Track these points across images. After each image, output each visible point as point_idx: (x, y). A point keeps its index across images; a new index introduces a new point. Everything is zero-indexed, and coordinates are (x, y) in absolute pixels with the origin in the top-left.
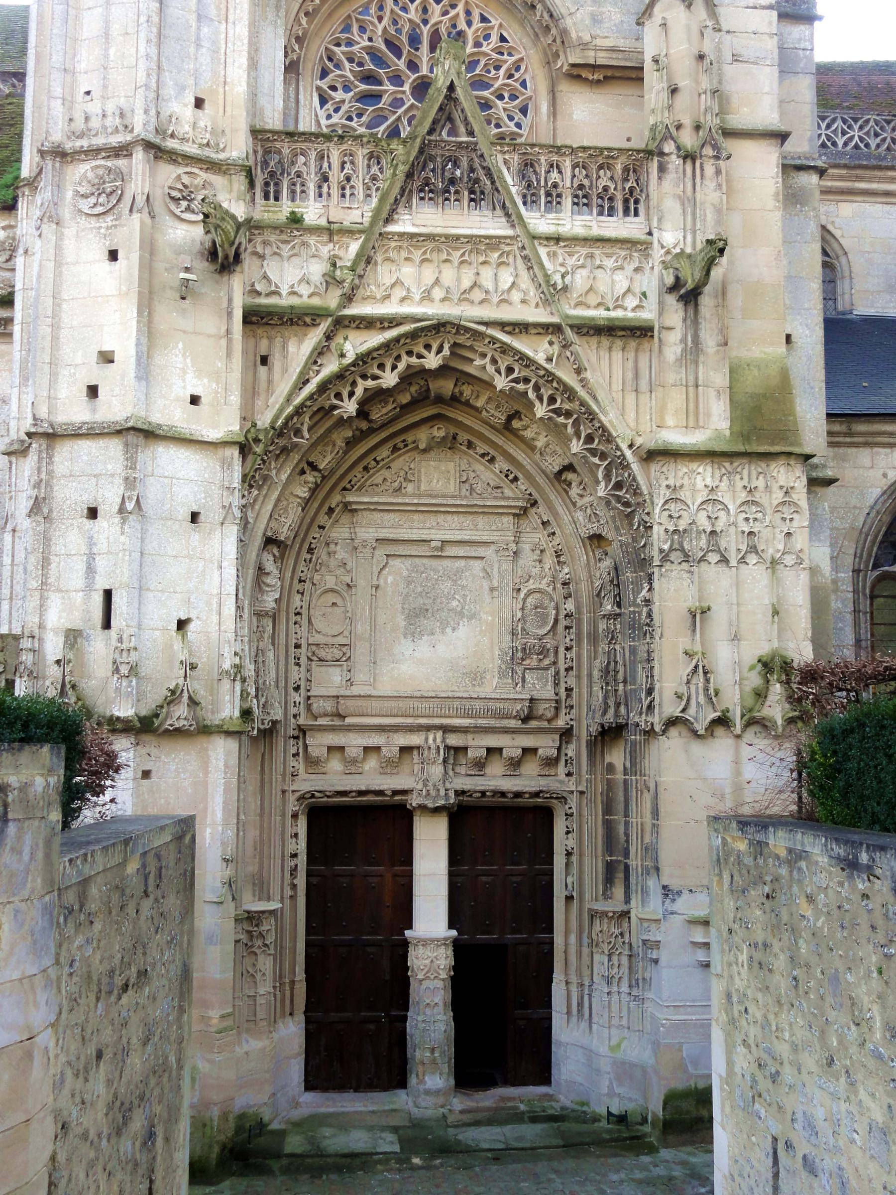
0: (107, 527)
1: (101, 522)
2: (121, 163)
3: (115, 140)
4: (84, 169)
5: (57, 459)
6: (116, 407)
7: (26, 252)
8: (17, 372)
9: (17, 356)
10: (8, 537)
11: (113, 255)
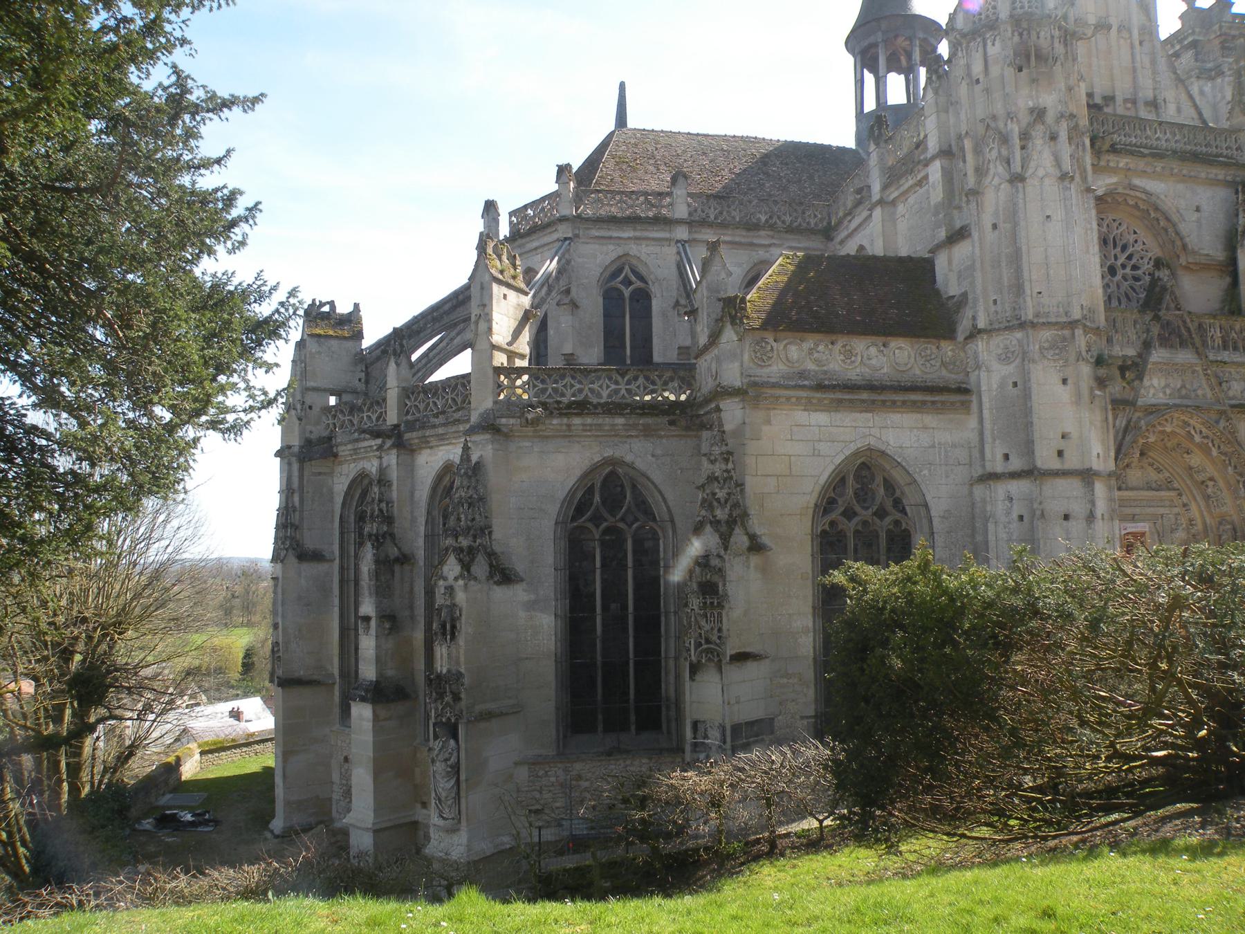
0: (1076, 526)
1: (1071, 523)
2: (1067, 332)
3: (1064, 319)
4: (1046, 334)
5: (1044, 488)
6: (1072, 462)
10: (991, 527)
11: (1065, 381)
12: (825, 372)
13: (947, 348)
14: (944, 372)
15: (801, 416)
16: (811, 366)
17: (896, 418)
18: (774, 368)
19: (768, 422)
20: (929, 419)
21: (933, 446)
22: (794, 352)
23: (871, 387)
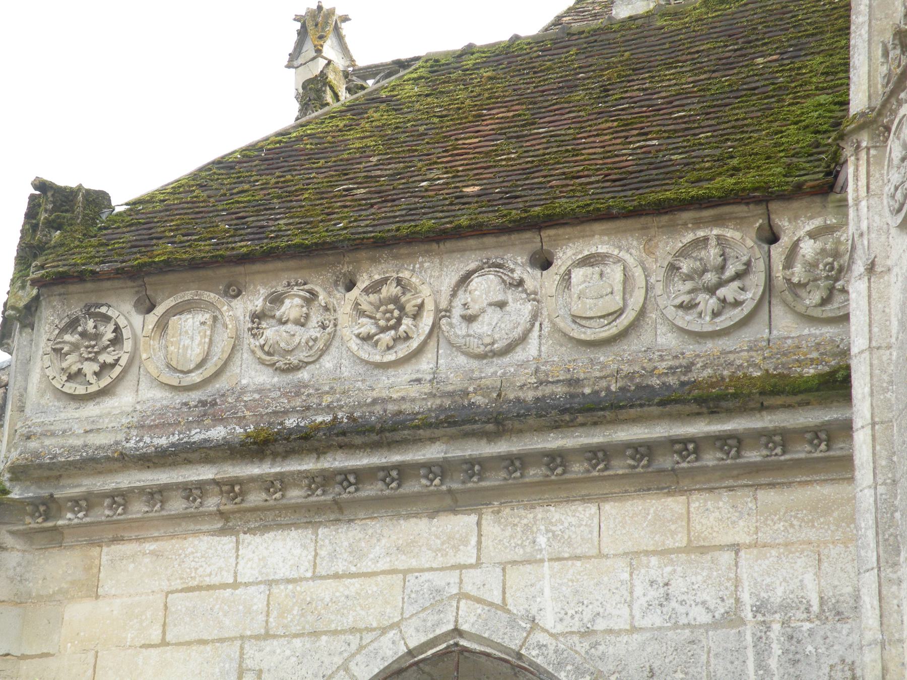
7: (871, 268)
8: (871, 534)
9: (866, 498)
12: (298, 389)
13: (799, 228)
14: (785, 326)
15: (208, 554)
16: (251, 375)
17: (573, 521)
18: (124, 400)
19: (93, 591)
20: (717, 514)
21: (731, 619)
22: (190, 335)
23: (456, 419)
